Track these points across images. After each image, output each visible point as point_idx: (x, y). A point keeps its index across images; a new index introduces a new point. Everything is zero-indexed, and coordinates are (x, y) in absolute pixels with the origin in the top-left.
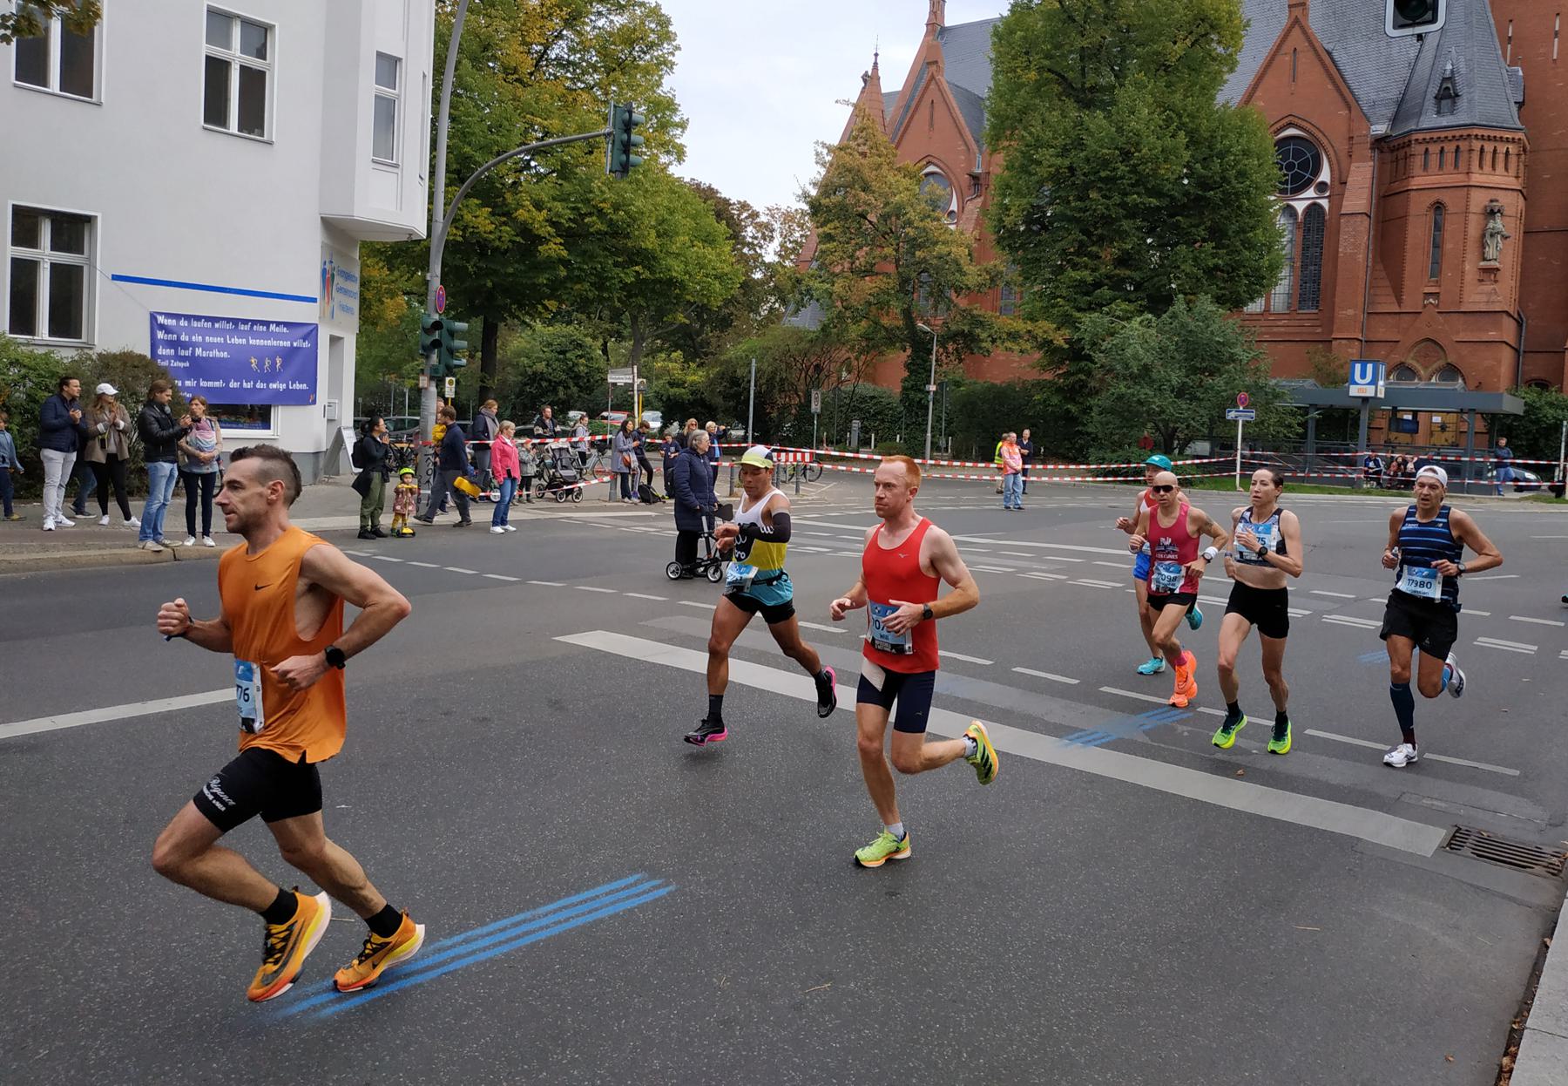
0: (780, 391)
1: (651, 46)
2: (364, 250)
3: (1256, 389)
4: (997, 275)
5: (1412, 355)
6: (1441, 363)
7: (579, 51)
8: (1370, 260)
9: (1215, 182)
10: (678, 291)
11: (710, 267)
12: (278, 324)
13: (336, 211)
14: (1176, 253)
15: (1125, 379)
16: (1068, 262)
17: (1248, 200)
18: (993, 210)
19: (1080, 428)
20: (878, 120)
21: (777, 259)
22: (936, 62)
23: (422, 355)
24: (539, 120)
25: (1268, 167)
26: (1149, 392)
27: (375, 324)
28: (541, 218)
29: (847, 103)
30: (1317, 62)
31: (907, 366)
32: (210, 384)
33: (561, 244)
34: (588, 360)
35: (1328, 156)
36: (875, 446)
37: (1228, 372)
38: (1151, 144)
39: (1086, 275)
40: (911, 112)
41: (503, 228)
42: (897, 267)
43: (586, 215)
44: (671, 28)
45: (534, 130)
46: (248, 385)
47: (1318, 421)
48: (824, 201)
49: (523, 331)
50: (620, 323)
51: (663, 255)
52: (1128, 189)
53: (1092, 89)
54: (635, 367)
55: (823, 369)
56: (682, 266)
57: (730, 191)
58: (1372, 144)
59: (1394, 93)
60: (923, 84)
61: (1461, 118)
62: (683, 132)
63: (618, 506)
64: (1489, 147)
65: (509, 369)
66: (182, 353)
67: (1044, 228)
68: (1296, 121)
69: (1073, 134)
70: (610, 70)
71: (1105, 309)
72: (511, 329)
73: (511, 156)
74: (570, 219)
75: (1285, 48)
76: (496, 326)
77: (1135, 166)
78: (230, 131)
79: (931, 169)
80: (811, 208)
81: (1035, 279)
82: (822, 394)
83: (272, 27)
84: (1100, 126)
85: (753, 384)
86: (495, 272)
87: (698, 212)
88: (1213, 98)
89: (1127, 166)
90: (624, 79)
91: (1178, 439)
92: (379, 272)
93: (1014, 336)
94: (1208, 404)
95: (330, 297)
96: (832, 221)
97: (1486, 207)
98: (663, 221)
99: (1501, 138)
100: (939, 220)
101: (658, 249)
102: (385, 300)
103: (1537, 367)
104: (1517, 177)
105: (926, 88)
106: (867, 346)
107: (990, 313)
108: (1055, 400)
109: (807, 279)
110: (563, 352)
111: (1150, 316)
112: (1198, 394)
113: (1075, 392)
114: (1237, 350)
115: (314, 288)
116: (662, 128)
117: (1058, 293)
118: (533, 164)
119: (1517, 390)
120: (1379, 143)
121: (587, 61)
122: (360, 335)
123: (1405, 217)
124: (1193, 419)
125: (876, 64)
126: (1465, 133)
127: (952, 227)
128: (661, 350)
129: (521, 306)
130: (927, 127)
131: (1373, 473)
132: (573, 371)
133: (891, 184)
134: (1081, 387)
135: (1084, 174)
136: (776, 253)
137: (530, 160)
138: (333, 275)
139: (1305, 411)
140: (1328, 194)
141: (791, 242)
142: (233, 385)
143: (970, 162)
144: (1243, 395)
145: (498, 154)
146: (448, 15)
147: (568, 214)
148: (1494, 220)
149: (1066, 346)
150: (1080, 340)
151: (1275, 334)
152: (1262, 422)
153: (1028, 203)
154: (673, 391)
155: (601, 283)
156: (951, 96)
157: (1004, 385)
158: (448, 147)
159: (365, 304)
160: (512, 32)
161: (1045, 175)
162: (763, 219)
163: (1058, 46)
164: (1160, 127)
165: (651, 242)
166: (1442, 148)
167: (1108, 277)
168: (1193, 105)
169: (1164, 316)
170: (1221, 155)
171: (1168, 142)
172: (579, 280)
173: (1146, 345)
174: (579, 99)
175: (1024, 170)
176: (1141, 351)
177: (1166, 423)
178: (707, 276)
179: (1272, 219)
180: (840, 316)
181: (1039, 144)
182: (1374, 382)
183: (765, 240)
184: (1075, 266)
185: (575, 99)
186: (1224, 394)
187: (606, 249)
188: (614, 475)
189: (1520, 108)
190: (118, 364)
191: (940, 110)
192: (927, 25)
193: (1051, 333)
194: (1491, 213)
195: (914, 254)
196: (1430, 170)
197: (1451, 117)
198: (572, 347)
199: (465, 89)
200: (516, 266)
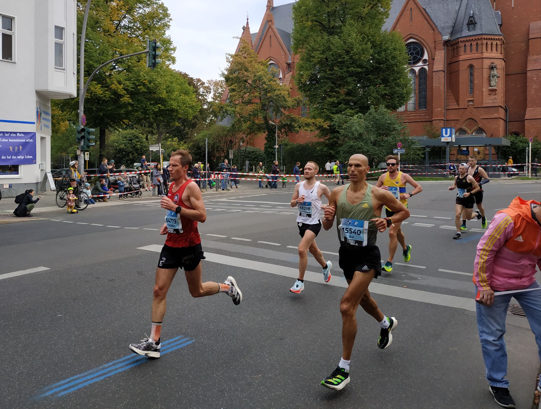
0: (218, 151)
1: (161, 19)
2: (52, 104)
3: (404, 141)
4: (299, 102)
5: (464, 125)
6: (476, 127)
7: (132, 23)
9: (383, 61)
10: (175, 113)
11: (187, 104)
13: (41, 88)
15: (352, 139)
16: (327, 95)
17: (396, 67)
18: (297, 76)
20: (250, 44)
21: (212, 100)
22: (271, 21)
24: (118, 50)
25: (404, 55)
26: (362, 143)
29: (237, 38)
30: (420, 13)
31: (266, 139)
33: (129, 97)
34: (141, 143)
35: (426, 49)
36: (255, 171)
37: (393, 135)
38: (357, 48)
39: (335, 100)
40: (262, 40)
41: (106, 92)
43: (138, 85)
44: (168, 12)
45: (116, 54)
47: (429, 152)
48: (231, 76)
49: (115, 132)
50: (153, 128)
51: (169, 100)
52: (349, 65)
53: (333, 27)
54: (160, 144)
56: (177, 104)
57: (193, 75)
59: (451, 24)
60: (266, 29)
62: (174, 52)
63: (157, 198)
65: (110, 148)
67: (317, 82)
68: (413, 36)
69: (327, 45)
70: (145, 30)
71: (343, 112)
72: (111, 131)
73: (108, 64)
74: (132, 87)
75: (407, 9)
77: (351, 56)
79: (271, 62)
81: (315, 102)
82: (234, 151)
83: (14, 18)
87: (182, 83)
88: (380, 28)
89: (348, 56)
90: (151, 33)
91: (375, 162)
92: (58, 112)
93: (307, 125)
95: (40, 122)
96: (234, 84)
97: (490, 66)
98: (168, 87)
100: (276, 81)
101: (167, 98)
103: (514, 127)
104: (501, 54)
105: (268, 30)
106: (250, 131)
107: (298, 116)
108: (325, 149)
109: (225, 107)
110: (131, 140)
111: (361, 114)
112: (382, 144)
113: (333, 145)
114: (396, 126)
115: (34, 119)
116: (166, 51)
117: (324, 107)
118: (116, 67)
119: (506, 137)
120: (446, 43)
124: (380, 154)
125: (248, 22)
126: (480, 37)
127: (281, 84)
128: (169, 137)
129: (114, 123)
130: (269, 46)
131: (453, 172)
132: (135, 147)
133: (256, 68)
136: (212, 98)
137: (116, 65)
138: (41, 113)
139: (424, 149)
140: (427, 64)
141: (218, 93)
143: (286, 58)
144: (399, 143)
145: (103, 63)
146: (81, 11)
148: (493, 70)
149: (328, 128)
151: (411, 119)
152: (408, 154)
153: (310, 73)
155: (145, 112)
156: (277, 33)
157: (304, 144)
159: (53, 125)
160: (107, 16)
161: (316, 62)
162: (206, 85)
163: (318, 12)
164: (361, 41)
165: (164, 95)
166: (471, 44)
167: (344, 100)
168: (373, 32)
169: (367, 114)
170: (385, 51)
171: (364, 46)
172: (137, 111)
173: (360, 126)
175: (308, 60)
176: (358, 128)
178: (186, 107)
180: (239, 121)
181: (314, 50)
182: (451, 136)
183: (208, 93)
184: (330, 97)
186: (392, 143)
187: (146, 98)
188: (154, 186)
189: (500, 27)
191: (273, 38)
192: (267, 7)
193: (322, 123)
194: (492, 68)
195: (266, 95)
196: (467, 53)
197: (474, 32)
198: (134, 138)
199: (89, 39)
200: (112, 107)
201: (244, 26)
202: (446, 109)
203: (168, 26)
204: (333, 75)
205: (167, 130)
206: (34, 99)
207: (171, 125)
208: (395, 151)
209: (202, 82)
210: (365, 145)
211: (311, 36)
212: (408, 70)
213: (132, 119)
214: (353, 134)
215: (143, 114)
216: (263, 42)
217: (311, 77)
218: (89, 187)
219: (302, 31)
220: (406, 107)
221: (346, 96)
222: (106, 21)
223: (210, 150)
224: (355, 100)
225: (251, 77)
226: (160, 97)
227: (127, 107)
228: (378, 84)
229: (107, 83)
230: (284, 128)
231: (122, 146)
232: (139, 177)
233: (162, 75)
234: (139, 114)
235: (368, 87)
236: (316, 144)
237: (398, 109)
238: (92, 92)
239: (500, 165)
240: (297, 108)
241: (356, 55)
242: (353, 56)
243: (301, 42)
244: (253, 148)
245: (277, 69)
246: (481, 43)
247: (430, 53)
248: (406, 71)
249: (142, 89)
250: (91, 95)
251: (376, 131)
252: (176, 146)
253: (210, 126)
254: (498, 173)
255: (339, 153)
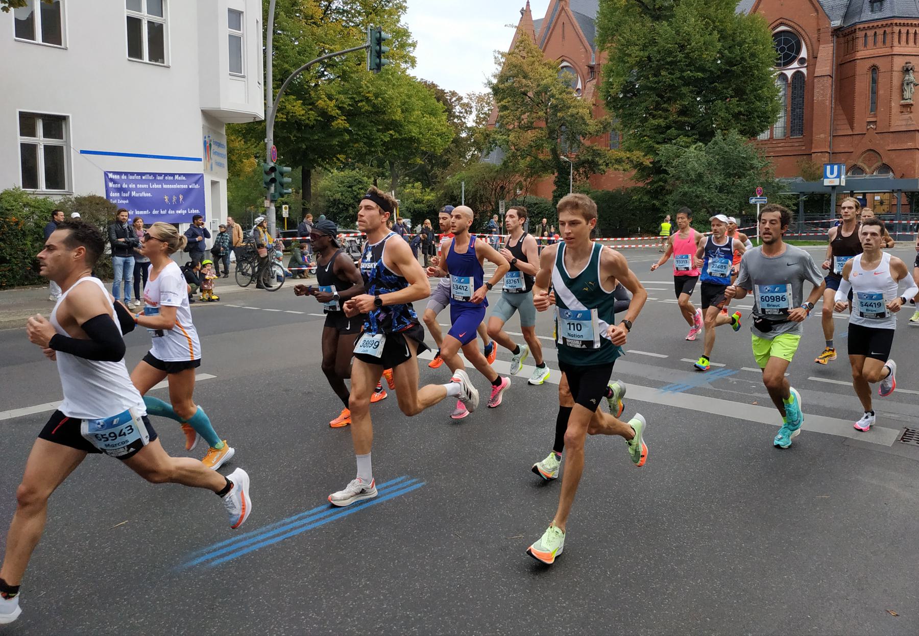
0: (481, 202)
3: (767, 185)
5: (860, 160)
6: (879, 164)
7: (350, 3)
8: (833, 103)
9: (737, 61)
10: (416, 145)
12: (180, 175)
13: (210, 106)
14: (715, 106)
16: (650, 114)
19: (662, 215)
20: (531, 37)
21: (474, 124)
23: (265, 187)
24: (328, 46)
25: (770, 50)
26: (701, 189)
27: (238, 175)
28: (332, 105)
29: (512, 26)
31: (555, 183)
32: (141, 212)
33: (345, 120)
35: (805, 42)
37: (750, 175)
38: (697, 40)
40: (551, 30)
41: (310, 112)
42: (547, 123)
43: (359, 101)
46: (164, 212)
47: (805, 202)
48: (500, 86)
50: (384, 168)
51: (406, 123)
52: (684, 68)
53: (659, 9)
55: (505, 188)
56: (418, 129)
58: (832, 32)
60: (558, 12)
61: (887, 13)
62: (414, 49)
64: (904, 30)
66: (124, 195)
67: (635, 95)
68: (785, 21)
69: (649, 36)
71: (674, 141)
76: (309, 172)
77: (688, 53)
78: (144, 61)
79: (565, 64)
80: (493, 91)
82: (505, 203)
84: (666, 30)
85: (463, 197)
86: (307, 139)
88: (734, 9)
90: (378, 19)
92: (239, 144)
93: (619, 161)
94: (738, 195)
99: (911, 24)
100: (570, 93)
101: (403, 120)
102: (244, 161)
105: (559, 15)
106: (531, 172)
108: (646, 199)
109: (493, 134)
110: (350, 187)
111: (701, 144)
112: (732, 189)
113: (658, 193)
114: (755, 162)
115: (200, 152)
117: (644, 134)
120: (837, 32)
121: (355, 9)
122: (229, 181)
123: (854, 76)
126: (889, 22)
129: (323, 160)
133: (541, 73)
134: (661, 190)
135: (657, 61)
136: (474, 121)
137: (325, 70)
138: (210, 145)
139: (798, 196)
140: (806, 65)
141: (482, 114)
142: (155, 212)
143: (588, 58)
147: (348, 101)
149: (651, 165)
150: (660, 161)
153: (624, 80)
154: (417, 206)
155: (370, 142)
157: (614, 191)
158: (274, 66)
159: (231, 164)
162: (465, 101)
164: (702, 29)
165: (398, 116)
166: (875, 32)
167: (675, 122)
168: (722, 14)
169: (709, 144)
170: (740, 45)
171: (708, 37)
172: (357, 141)
174: (351, 32)
175: (621, 60)
177: (711, 207)
178: (433, 135)
179: (772, 82)
180: (514, 156)
181: (629, 43)
182: (839, 176)
183: (467, 113)
184: (654, 117)
185: (348, 33)
187: (371, 122)
190: (87, 203)
191: (568, 28)
194: (906, 71)
195: (556, 115)
198: (355, 183)
199: (282, 30)
200: (319, 135)
201: (523, 8)
202: (833, 136)
203: (405, 9)
204: (658, 84)
205: (406, 169)
206: (198, 123)
207: (409, 162)
208: (752, 201)
209: (459, 97)
210: (706, 192)
211: (626, 22)
212: (776, 74)
213: (351, 153)
214: (688, 174)
215: (368, 146)
216: (551, 33)
217: (625, 86)
218: (281, 258)
219: (612, 15)
220: (772, 133)
221: (679, 117)
222: (308, 2)
223: (471, 201)
224: (693, 122)
225: (532, 87)
226: (393, 120)
227: (342, 135)
228: (728, 97)
229: (311, 99)
230: (584, 167)
231: (338, 196)
232: (361, 242)
233: (394, 85)
234: (359, 146)
235: (713, 101)
236: (632, 191)
237: (758, 134)
238: (288, 113)
239: (914, 222)
240: (604, 135)
241: (695, 51)
242: (690, 53)
243: (609, 32)
244: (535, 197)
245: (573, 75)
246: (890, 31)
247: (810, 48)
248: (772, 76)
249: (365, 107)
250: (287, 115)
251: (724, 169)
252: (419, 196)
253: (470, 164)
254: (909, 233)
255: (667, 205)
